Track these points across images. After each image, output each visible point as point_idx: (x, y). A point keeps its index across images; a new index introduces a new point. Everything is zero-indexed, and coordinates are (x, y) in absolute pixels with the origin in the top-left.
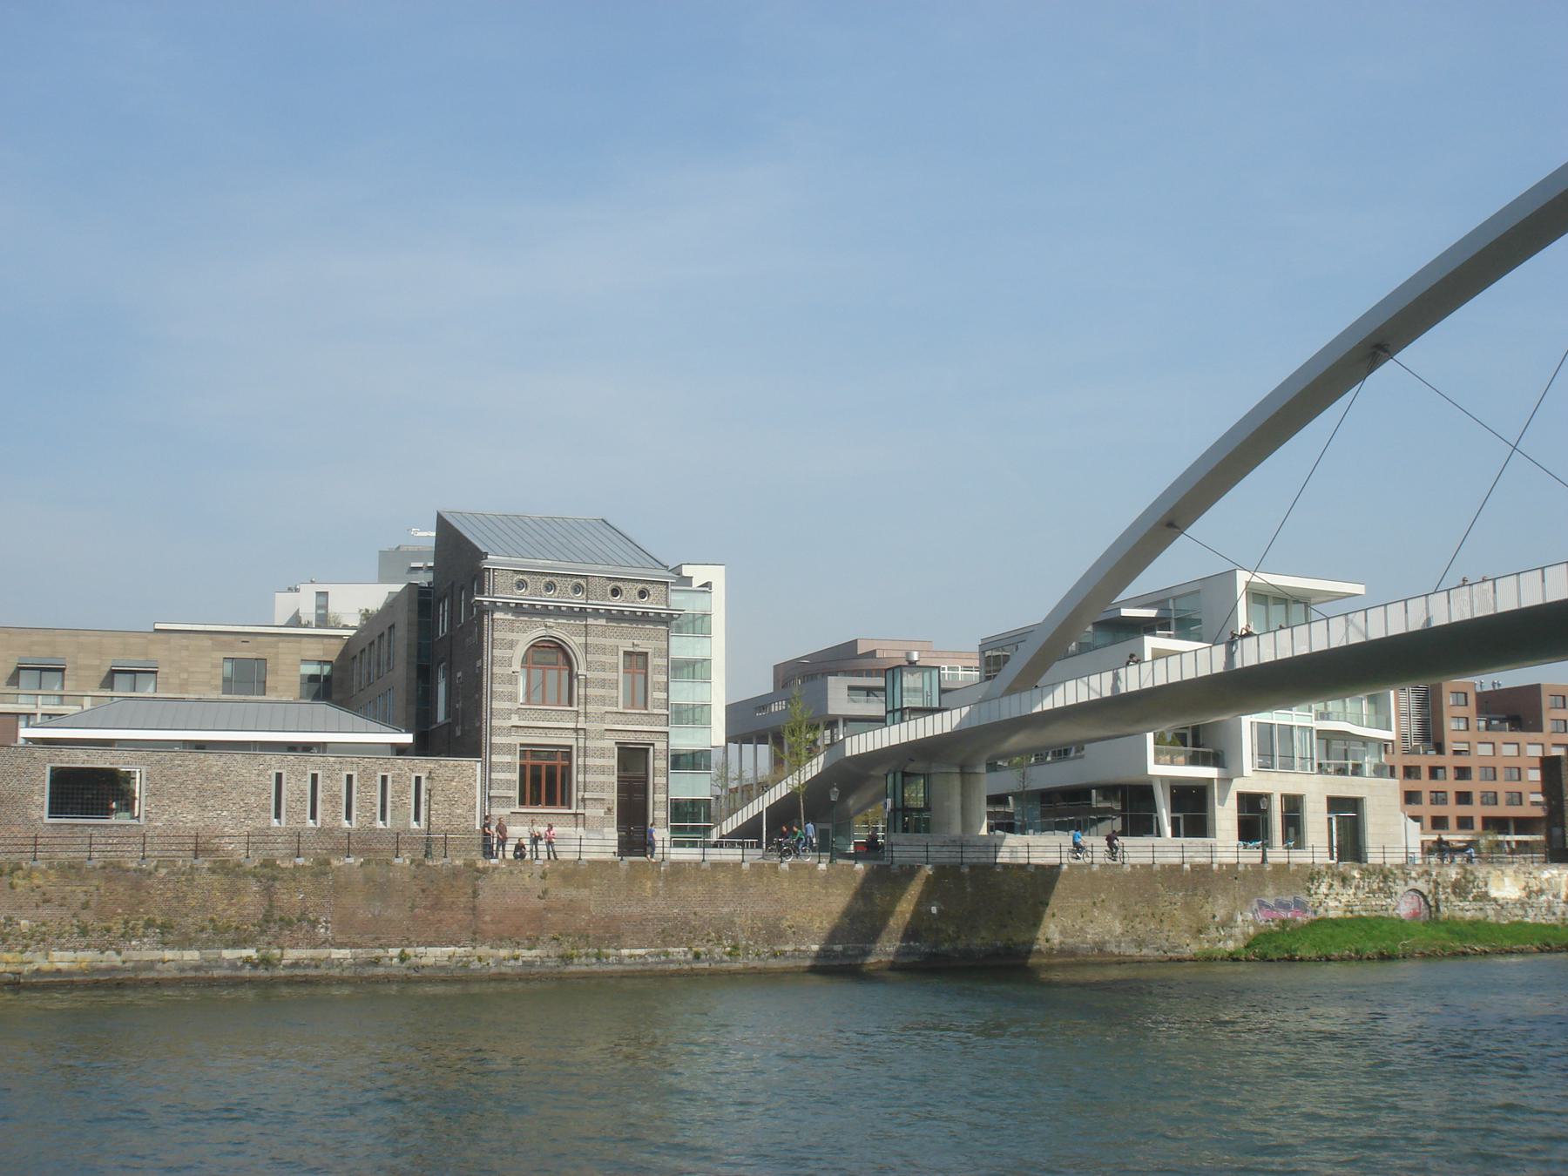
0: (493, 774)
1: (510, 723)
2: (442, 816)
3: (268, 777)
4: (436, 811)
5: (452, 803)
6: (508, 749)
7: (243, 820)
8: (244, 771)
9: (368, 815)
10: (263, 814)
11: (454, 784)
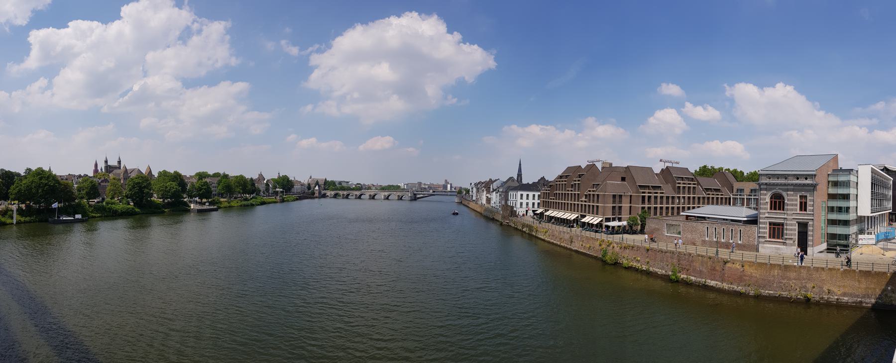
1: (765, 216)
5: (749, 237)
6: (764, 223)
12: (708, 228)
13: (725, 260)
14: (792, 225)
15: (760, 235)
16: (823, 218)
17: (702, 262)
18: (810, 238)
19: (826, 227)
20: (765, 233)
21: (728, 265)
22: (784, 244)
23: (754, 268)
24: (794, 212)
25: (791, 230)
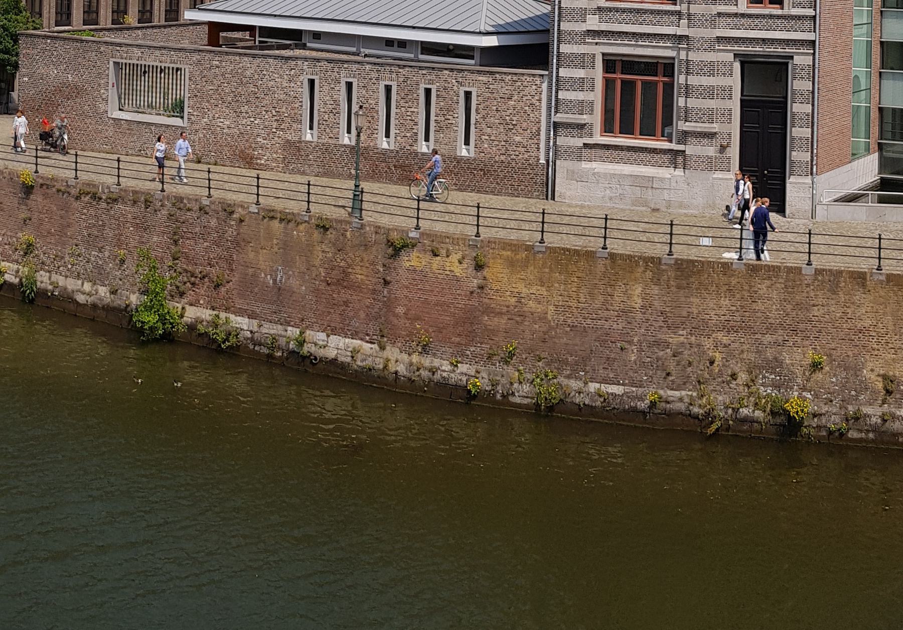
0: (560, 93)
1: (584, 27)
2: (497, 143)
3: (299, 83)
4: (489, 136)
5: (510, 127)
6: (583, 61)
7: (274, 130)
8: (276, 75)
9: (408, 135)
10: (295, 125)
11: (513, 103)
12: (312, 83)
13: (394, 236)
14: (711, 69)
15: (559, 117)
16: (860, 36)
17: (286, 246)
18: (797, 132)
19: (875, 77)
20: (583, 107)
21: (412, 260)
22: (676, 158)
23: (531, 273)
24: (723, 8)
25: (710, 93)
